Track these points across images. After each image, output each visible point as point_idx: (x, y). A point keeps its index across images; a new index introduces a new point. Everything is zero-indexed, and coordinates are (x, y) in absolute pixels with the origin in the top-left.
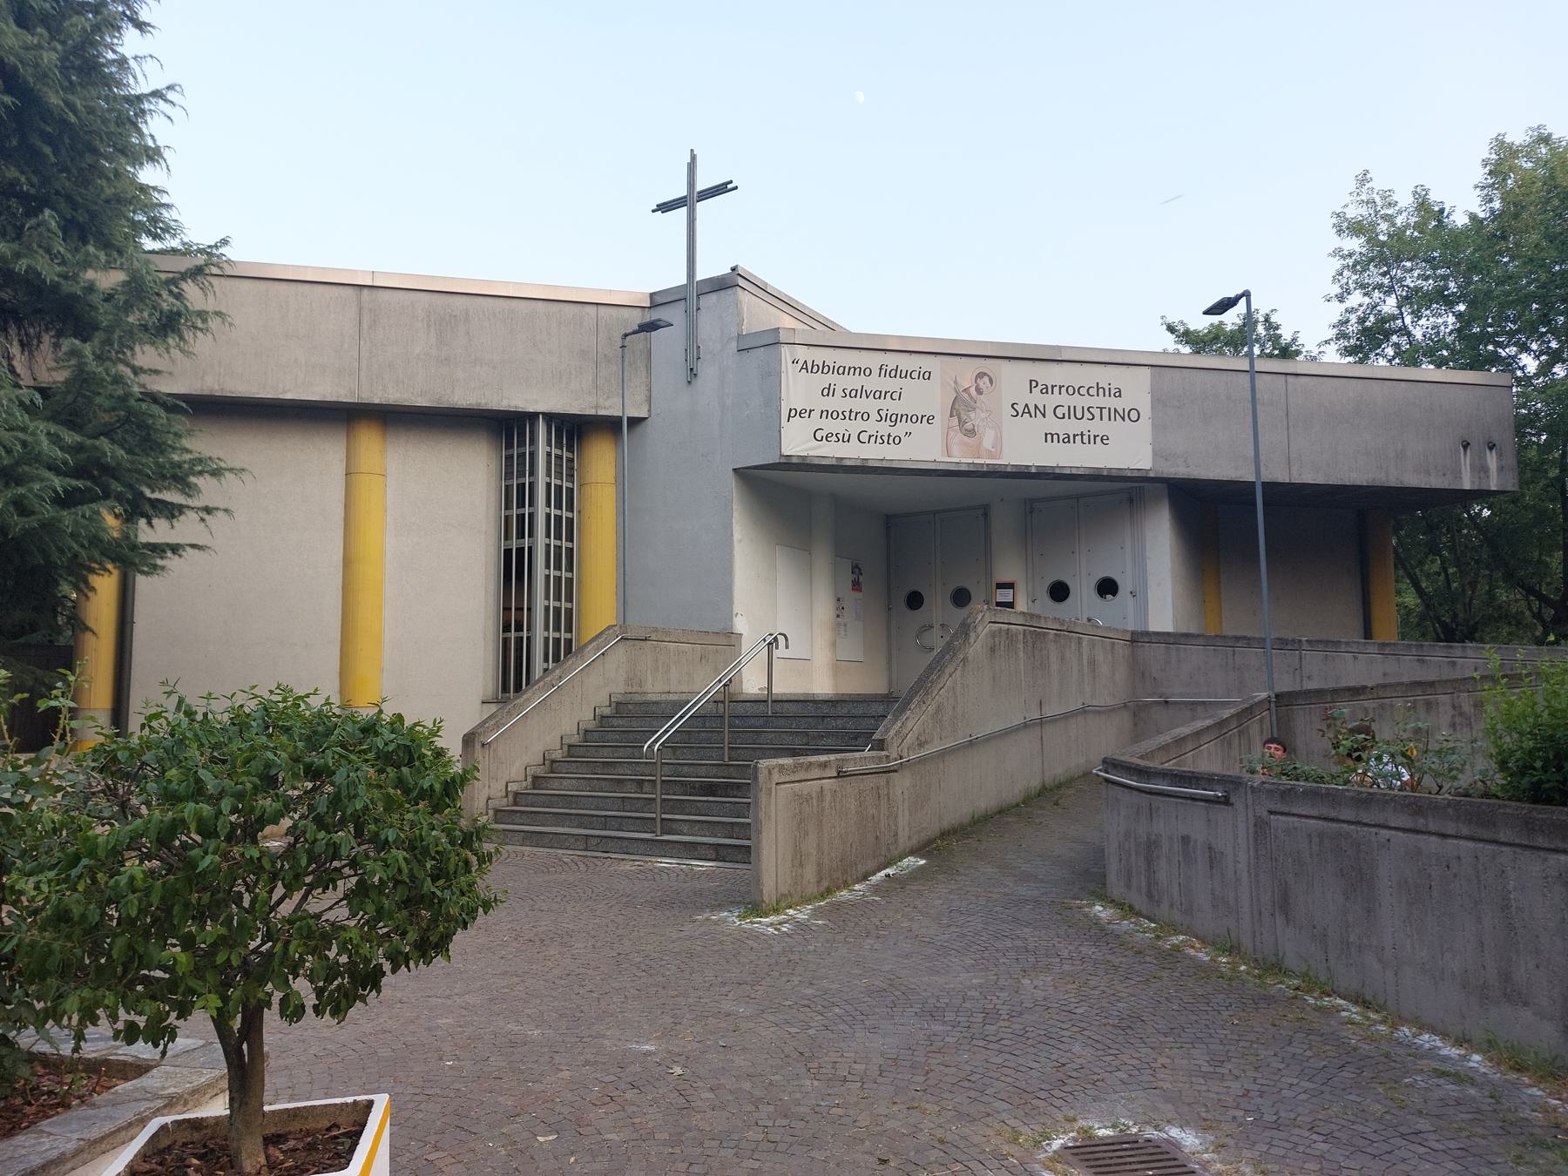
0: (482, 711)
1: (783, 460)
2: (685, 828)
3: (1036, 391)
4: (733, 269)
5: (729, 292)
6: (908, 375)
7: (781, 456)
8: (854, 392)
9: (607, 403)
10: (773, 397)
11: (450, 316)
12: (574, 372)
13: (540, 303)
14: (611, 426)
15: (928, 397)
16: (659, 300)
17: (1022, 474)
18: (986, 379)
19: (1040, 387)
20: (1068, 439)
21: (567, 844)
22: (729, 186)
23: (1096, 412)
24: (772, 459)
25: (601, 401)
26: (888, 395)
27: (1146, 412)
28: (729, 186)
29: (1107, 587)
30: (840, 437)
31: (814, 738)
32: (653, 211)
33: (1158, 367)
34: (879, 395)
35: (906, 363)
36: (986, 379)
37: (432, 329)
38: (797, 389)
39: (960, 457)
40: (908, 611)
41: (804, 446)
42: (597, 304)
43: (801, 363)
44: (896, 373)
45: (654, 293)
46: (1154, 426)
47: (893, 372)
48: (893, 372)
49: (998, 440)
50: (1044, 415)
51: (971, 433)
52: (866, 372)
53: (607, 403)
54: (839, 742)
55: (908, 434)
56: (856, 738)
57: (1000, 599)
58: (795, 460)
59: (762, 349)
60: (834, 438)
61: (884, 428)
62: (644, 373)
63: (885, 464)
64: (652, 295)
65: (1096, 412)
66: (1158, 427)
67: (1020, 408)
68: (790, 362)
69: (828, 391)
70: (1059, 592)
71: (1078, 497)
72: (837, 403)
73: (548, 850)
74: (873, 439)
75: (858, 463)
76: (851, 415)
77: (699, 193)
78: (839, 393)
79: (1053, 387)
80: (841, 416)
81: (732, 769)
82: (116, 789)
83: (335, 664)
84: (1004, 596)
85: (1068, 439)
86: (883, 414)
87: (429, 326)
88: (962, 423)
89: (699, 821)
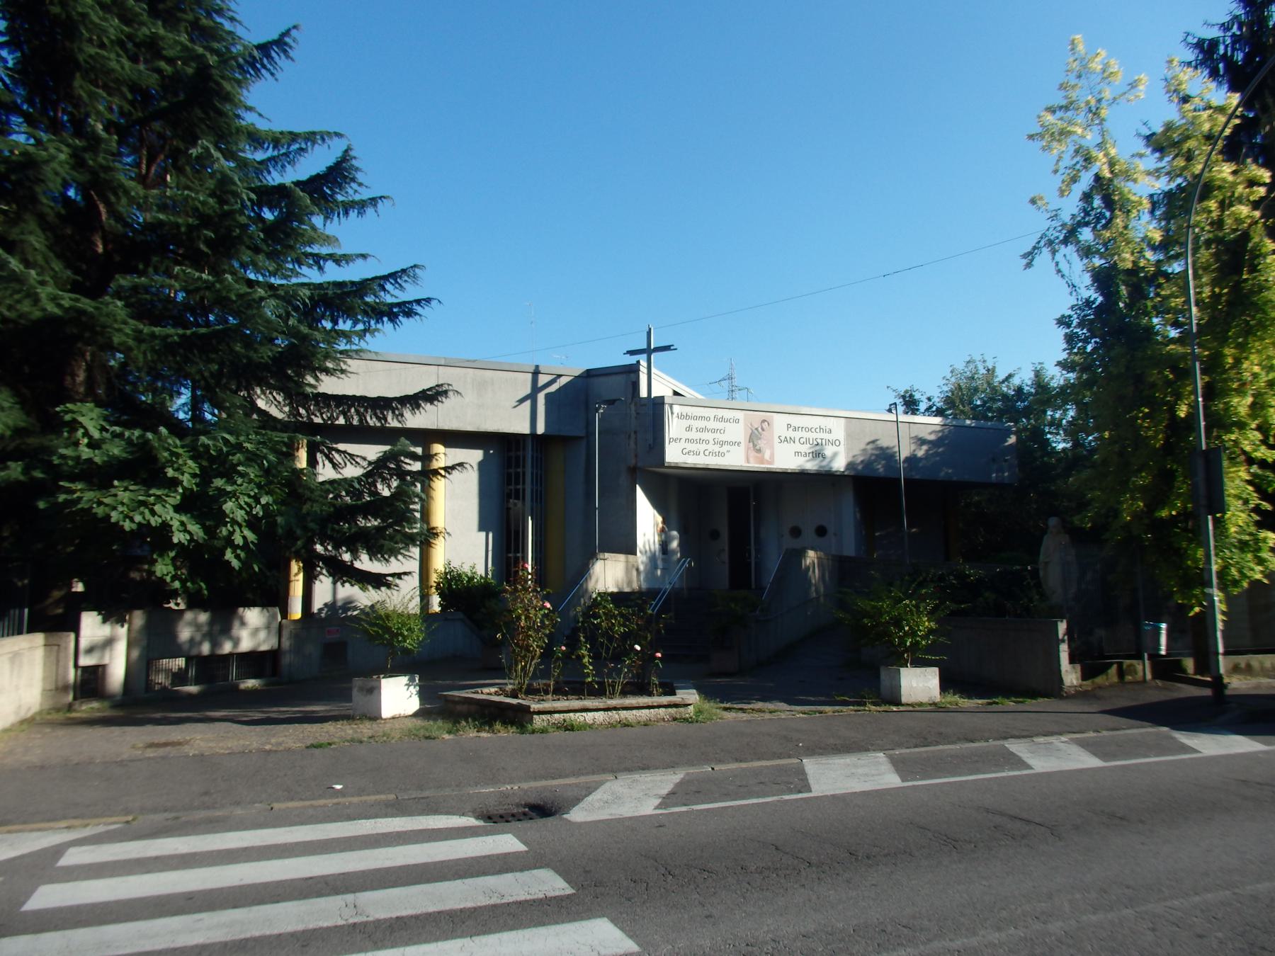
3: (790, 429)
6: (728, 421)
27: (842, 443)
34: (714, 431)
39: (754, 465)
44: (722, 419)
49: (772, 455)
52: (708, 419)
55: (728, 451)
61: (717, 448)
67: (783, 438)
69: (689, 429)
72: (694, 435)
76: (701, 441)
78: (694, 430)
88: (754, 446)
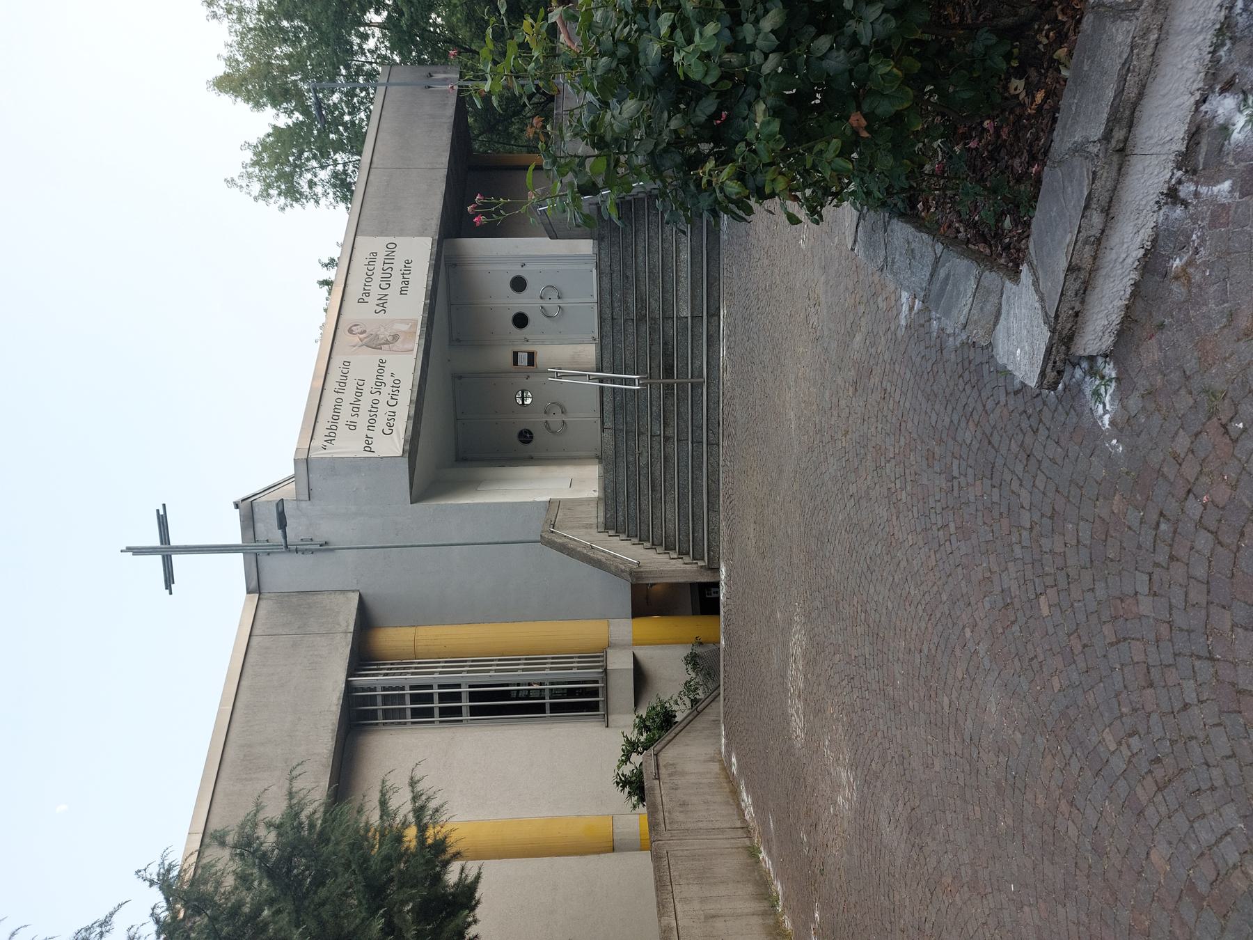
0: (616, 727)
1: (407, 455)
2: (697, 363)
3: (366, 299)
4: (237, 506)
5: (256, 510)
6: (345, 375)
7: (403, 456)
8: (355, 409)
9: (344, 624)
10: (353, 465)
11: (243, 760)
12: (311, 653)
13: (242, 683)
14: (365, 622)
15: (364, 364)
16: (254, 584)
17: (431, 309)
18: (354, 328)
19: (364, 297)
20: (406, 282)
21: (715, 464)
22: (161, 513)
23: (386, 266)
24: (404, 465)
25: (340, 630)
26: (359, 387)
27: (391, 239)
28: (161, 513)
29: (519, 284)
30: (390, 418)
31: (628, 314)
32: (171, 593)
33: (357, 230)
34: (359, 393)
35: (335, 375)
36: (354, 328)
37: (254, 776)
38: (348, 446)
39: (415, 344)
40: (530, 323)
41: (396, 441)
42: (250, 636)
43: (325, 444)
44: (342, 383)
45: (247, 589)
46: (401, 235)
47: (341, 384)
48: (341, 384)
49: (402, 321)
50: (386, 295)
51: (395, 338)
52: (339, 402)
53: (344, 624)
54: (630, 292)
55: (392, 375)
56: (627, 277)
57: (525, 363)
58: (407, 447)
59: (311, 476)
60: (391, 422)
61: (386, 390)
62: (319, 596)
63: (416, 389)
64: (248, 592)
65: (386, 266)
66: (402, 233)
67: (379, 309)
68: (325, 451)
69: (352, 426)
70: (521, 320)
71: (450, 304)
72: (363, 420)
73: (721, 484)
74: (394, 397)
75: (413, 406)
76: (373, 411)
77: (162, 543)
78: (354, 419)
79: (365, 290)
80: (374, 417)
81: (653, 365)
82: (673, 28)
83: (572, 861)
84: (523, 359)
85: (406, 282)
86: (374, 391)
87: (251, 779)
88: (387, 342)
89: (692, 350)
